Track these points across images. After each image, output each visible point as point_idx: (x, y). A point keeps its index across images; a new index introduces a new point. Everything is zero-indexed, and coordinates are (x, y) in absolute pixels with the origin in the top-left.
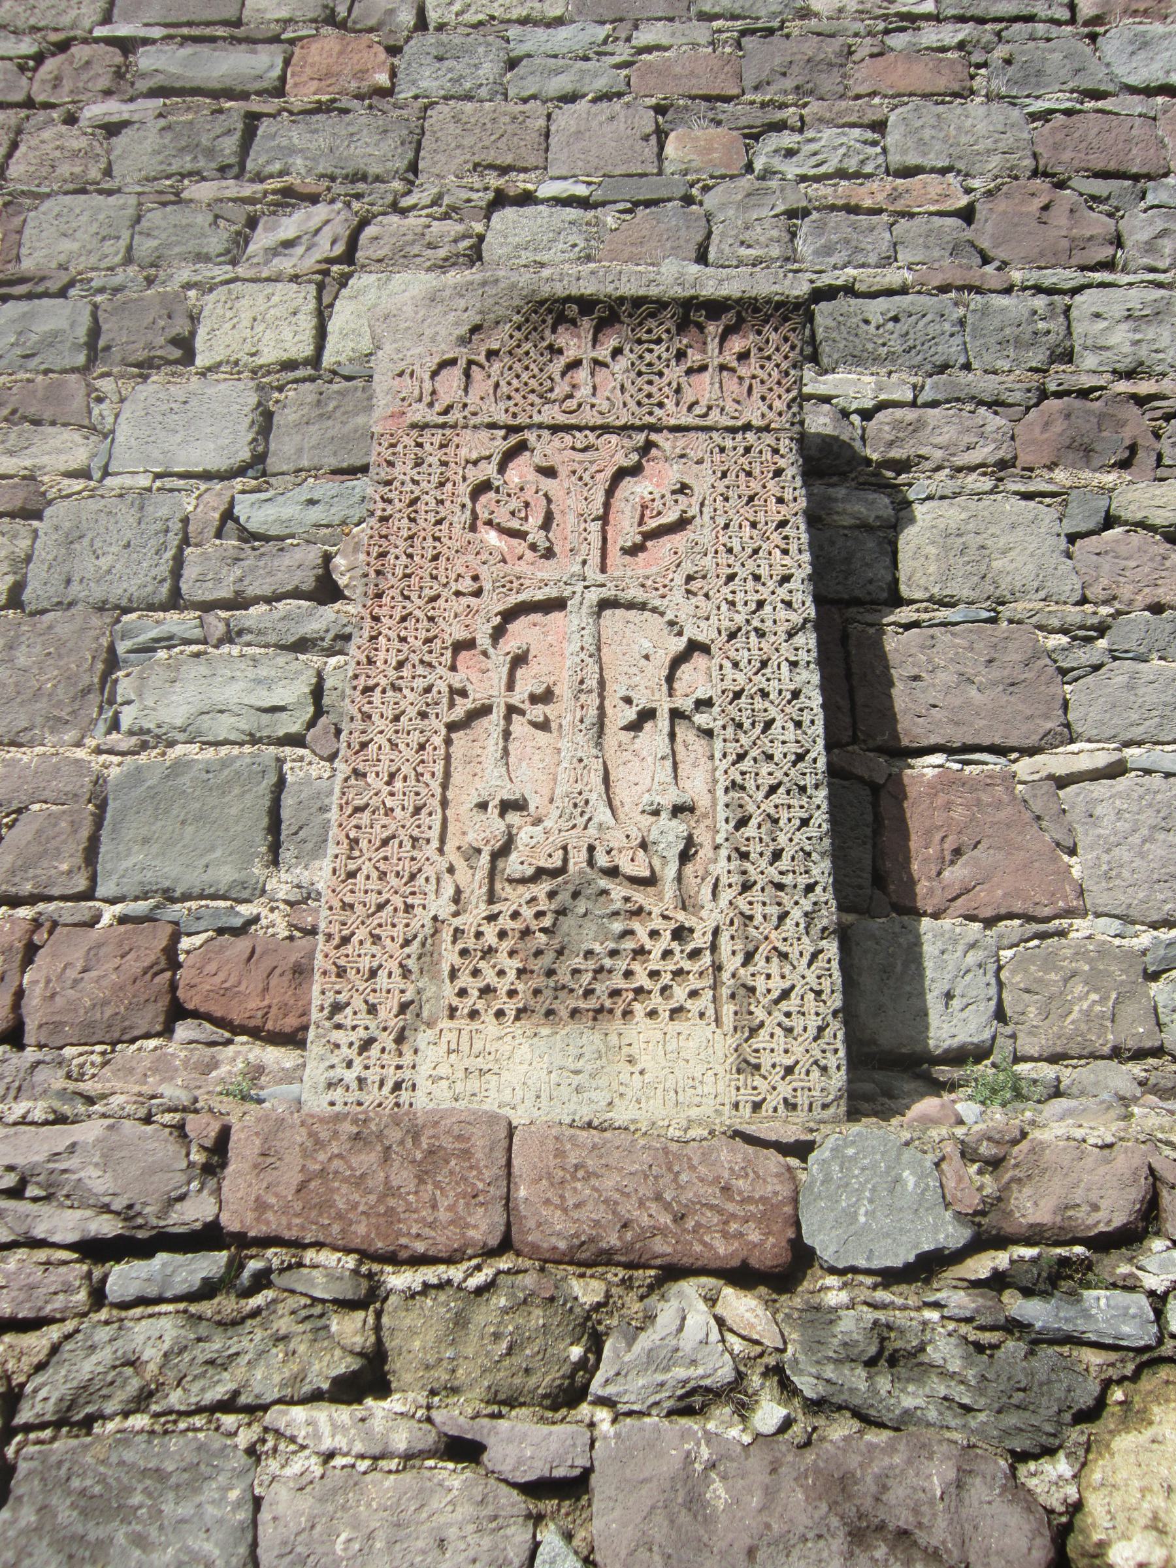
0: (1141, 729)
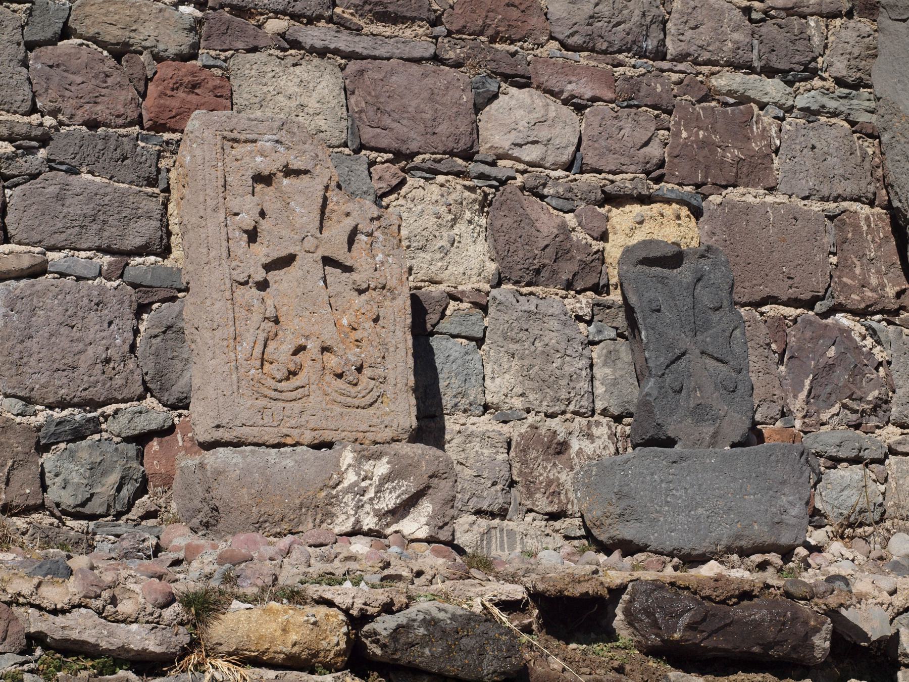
0: (63, 236)
